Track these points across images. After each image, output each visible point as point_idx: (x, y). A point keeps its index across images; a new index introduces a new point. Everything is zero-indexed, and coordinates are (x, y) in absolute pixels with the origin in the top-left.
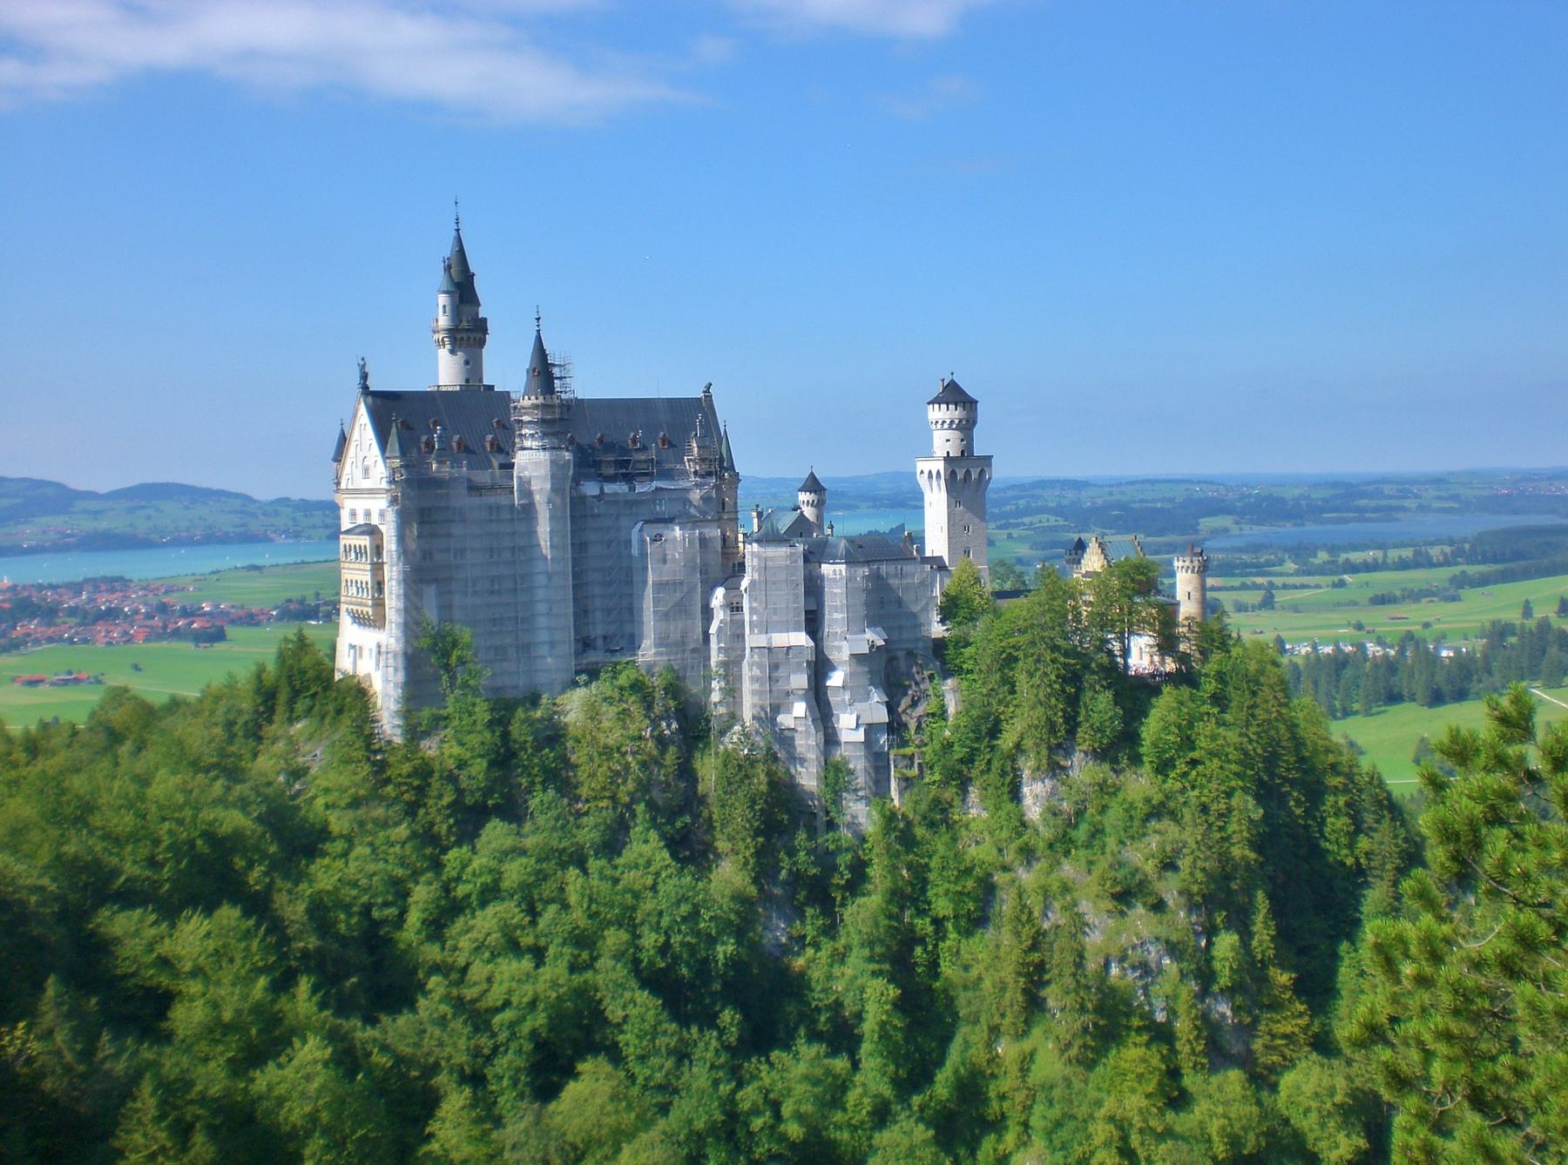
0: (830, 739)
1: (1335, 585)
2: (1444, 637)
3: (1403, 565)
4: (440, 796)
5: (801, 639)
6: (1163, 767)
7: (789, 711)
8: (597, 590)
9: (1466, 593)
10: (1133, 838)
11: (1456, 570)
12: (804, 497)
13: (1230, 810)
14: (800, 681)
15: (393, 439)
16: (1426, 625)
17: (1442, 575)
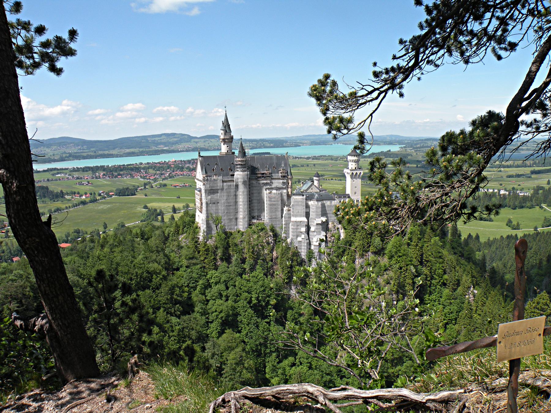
0: (310, 244)
1: (498, 171)
2: (523, 189)
3: (518, 166)
4: (211, 257)
5: (305, 219)
6: (391, 257)
7: (301, 237)
8: (256, 205)
9: (533, 176)
10: (381, 275)
11: (532, 169)
12: (315, 178)
13: (407, 269)
14: (303, 229)
15: (204, 169)
16: (519, 185)
17: (528, 170)
